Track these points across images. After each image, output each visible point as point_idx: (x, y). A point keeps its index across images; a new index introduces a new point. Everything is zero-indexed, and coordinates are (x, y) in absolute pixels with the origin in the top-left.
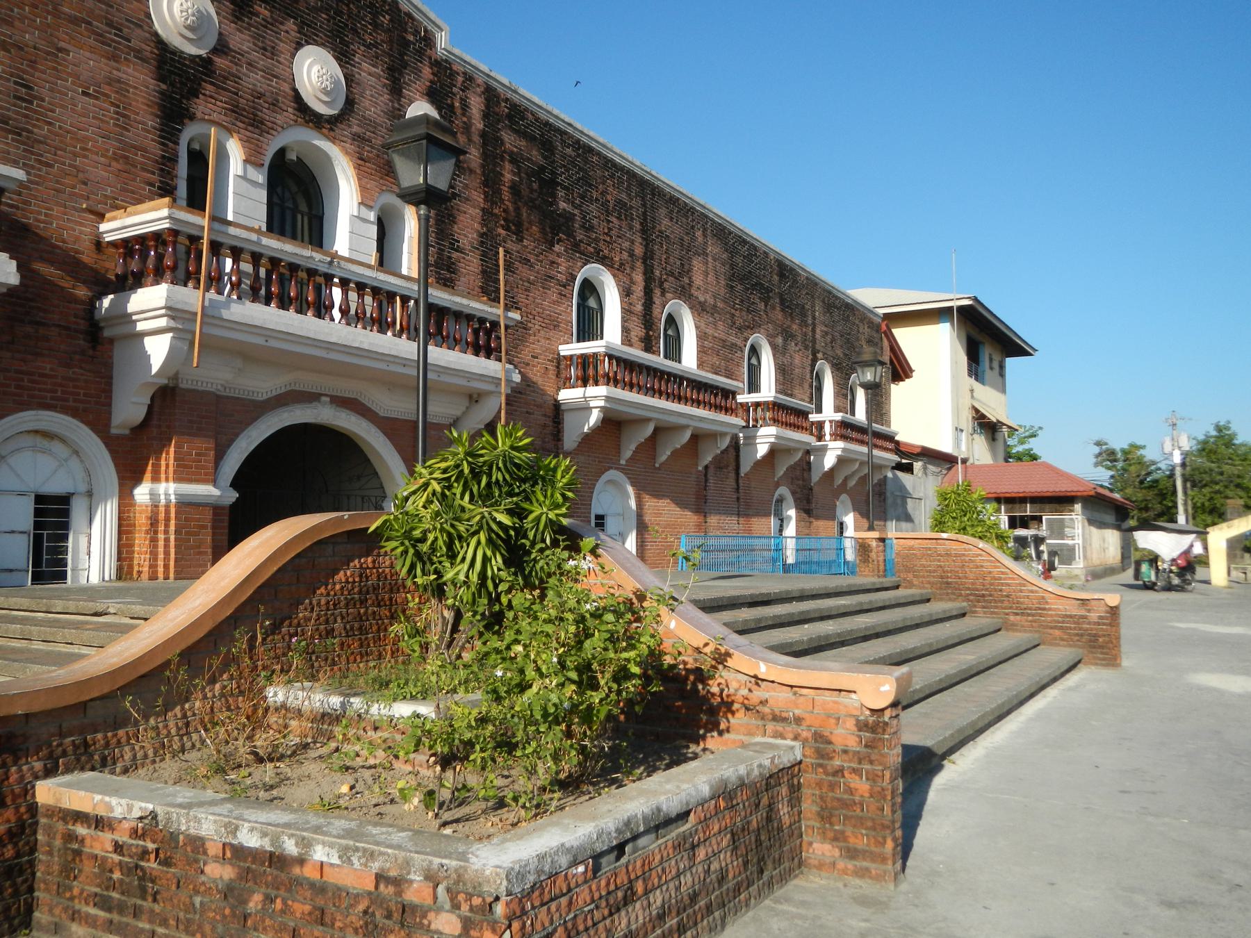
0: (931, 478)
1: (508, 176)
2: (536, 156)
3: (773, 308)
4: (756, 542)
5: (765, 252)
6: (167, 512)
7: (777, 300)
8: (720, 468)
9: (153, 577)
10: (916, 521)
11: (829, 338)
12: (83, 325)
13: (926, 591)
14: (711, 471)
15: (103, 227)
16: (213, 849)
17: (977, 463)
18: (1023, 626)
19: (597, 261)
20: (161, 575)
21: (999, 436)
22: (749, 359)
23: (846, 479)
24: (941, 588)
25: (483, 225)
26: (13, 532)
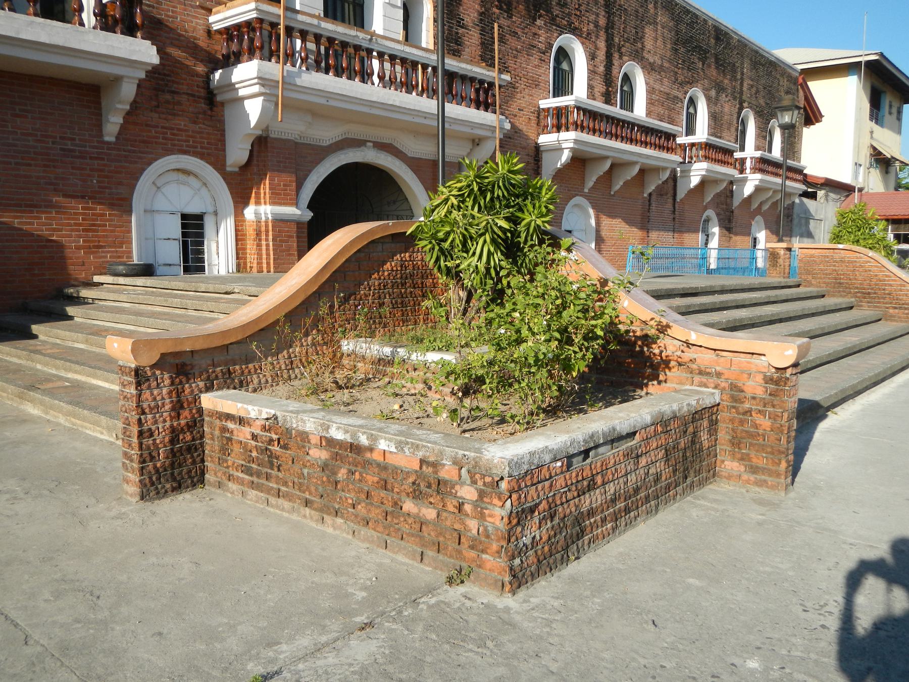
0: (831, 203)
3: (709, 66)
4: (687, 252)
5: (704, 20)
6: (267, 226)
7: (713, 60)
8: (662, 195)
9: (260, 271)
11: (754, 90)
12: (202, 93)
13: (822, 289)
14: (654, 197)
15: (212, 19)
16: (314, 440)
17: (871, 191)
18: (900, 317)
19: (570, 32)
20: (265, 270)
21: (892, 169)
22: (688, 109)
23: (761, 204)
24: (834, 287)
25: (482, 6)
26: (169, 239)
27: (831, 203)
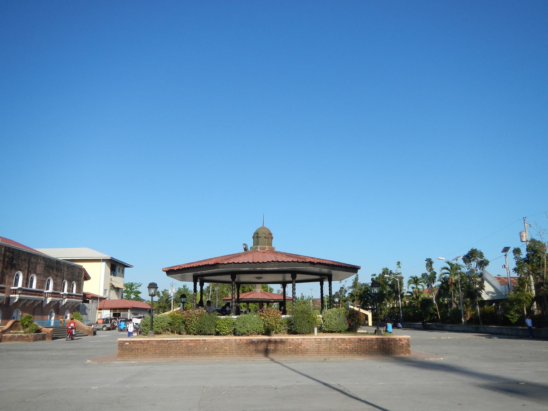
0: (94, 303)
1: (6, 260)
2: (11, 255)
3: (54, 271)
7: (55, 269)
10: (88, 315)
11: (67, 274)
17: (111, 299)
23: (68, 306)
27: (94, 303)
